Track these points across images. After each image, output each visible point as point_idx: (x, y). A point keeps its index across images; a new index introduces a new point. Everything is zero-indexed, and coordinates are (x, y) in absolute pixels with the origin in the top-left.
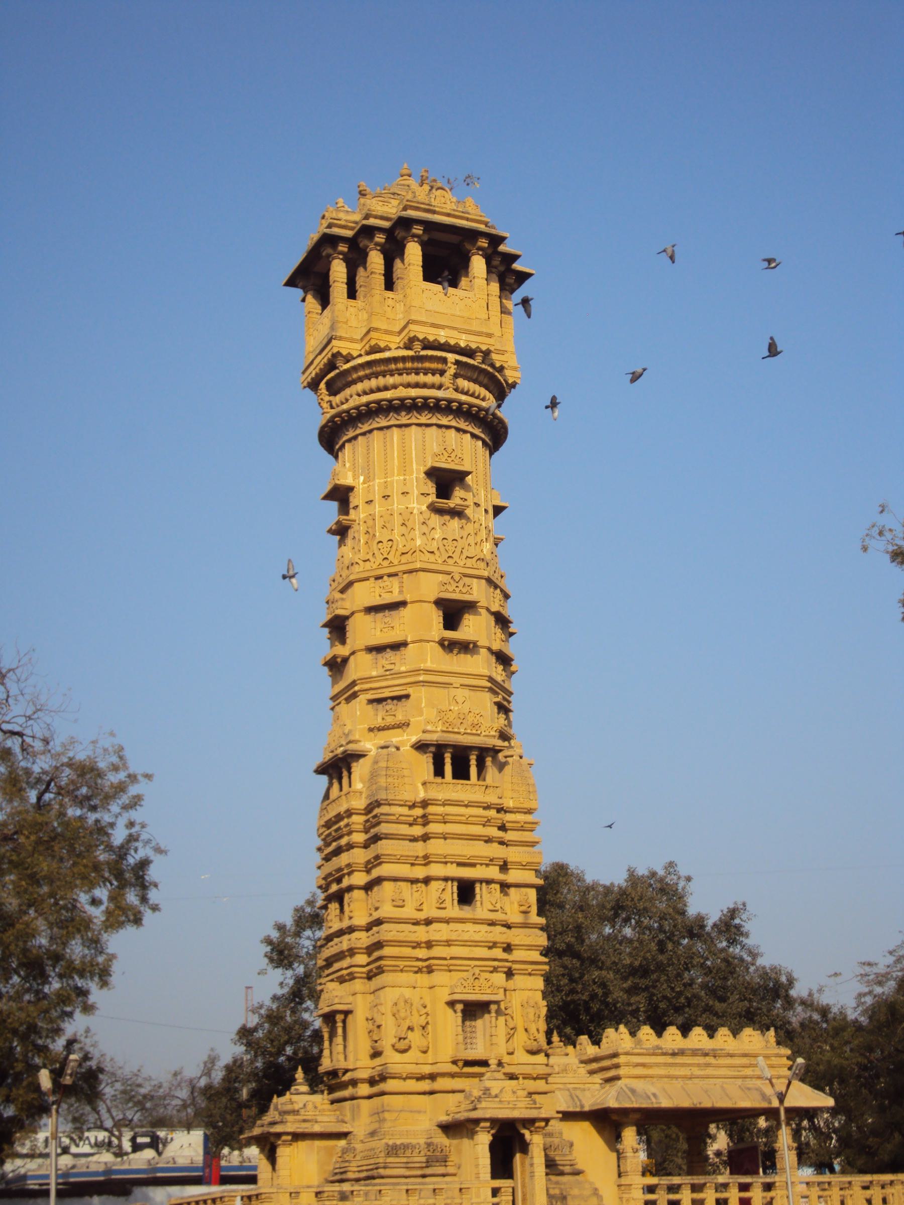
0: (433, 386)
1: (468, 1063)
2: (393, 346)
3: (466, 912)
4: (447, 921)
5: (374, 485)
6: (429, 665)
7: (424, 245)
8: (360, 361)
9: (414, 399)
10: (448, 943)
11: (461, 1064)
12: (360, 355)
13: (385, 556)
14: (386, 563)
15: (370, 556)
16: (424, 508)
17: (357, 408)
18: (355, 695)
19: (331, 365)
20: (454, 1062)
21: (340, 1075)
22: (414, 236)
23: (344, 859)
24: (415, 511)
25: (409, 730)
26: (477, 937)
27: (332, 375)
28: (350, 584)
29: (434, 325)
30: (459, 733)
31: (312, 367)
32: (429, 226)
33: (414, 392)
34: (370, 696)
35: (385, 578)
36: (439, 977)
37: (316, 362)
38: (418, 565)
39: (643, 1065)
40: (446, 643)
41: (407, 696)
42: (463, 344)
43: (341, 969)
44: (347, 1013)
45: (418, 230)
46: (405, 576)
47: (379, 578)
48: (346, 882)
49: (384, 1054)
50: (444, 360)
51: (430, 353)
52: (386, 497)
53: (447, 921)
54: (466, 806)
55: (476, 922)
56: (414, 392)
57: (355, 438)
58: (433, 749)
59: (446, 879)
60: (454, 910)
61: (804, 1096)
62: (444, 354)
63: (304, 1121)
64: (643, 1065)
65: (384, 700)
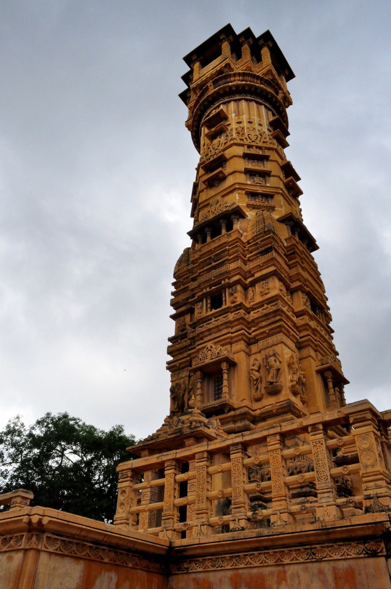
5: (243, 118)
10: (314, 331)
13: (253, 140)
15: (244, 138)
18: (231, 192)
21: (226, 411)
28: (231, 146)
35: (254, 147)
44: (232, 365)
46: (266, 150)
49: (283, 392)
52: (250, 122)
57: (229, 102)
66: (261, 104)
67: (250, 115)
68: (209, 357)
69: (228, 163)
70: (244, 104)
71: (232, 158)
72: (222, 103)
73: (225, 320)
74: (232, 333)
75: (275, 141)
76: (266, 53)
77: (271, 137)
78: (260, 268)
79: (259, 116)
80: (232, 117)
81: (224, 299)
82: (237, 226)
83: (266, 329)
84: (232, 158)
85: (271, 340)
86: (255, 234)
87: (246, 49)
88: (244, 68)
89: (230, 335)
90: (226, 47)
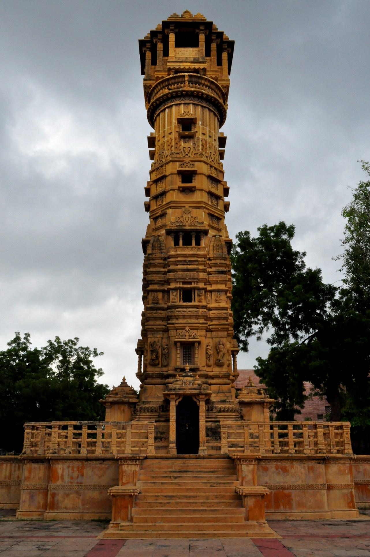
15: (208, 155)
17: (208, 95)
18: (199, 208)
19: (196, 71)
23: (202, 275)
27: (195, 74)
31: (181, 64)
37: (185, 64)
43: (198, 323)
44: (199, 343)
47: (211, 166)
48: (193, 285)
57: (198, 105)
67: (210, 129)
68: (187, 336)
69: (196, 176)
70: (207, 112)
71: (201, 174)
72: (193, 104)
73: (195, 314)
74: (201, 324)
78: (217, 282)
80: (199, 123)
81: (193, 296)
82: (204, 242)
83: (220, 327)
84: (201, 174)
85: (220, 334)
86: (215, 256)
87: (214, 46)
88: (214, 76)
89: (201, 325)
90: (202, 37)
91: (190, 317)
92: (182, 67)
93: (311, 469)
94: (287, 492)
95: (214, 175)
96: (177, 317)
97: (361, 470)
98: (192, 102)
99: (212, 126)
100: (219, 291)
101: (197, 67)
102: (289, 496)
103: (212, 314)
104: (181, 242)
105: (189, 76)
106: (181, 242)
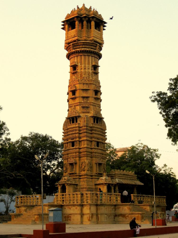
0: (94, 49)
1: (99, 174)
2: (88, 40)
3: (98, 148)
4: (95, 149)
6: (93, 102)
7: (95, 22)
8: (82, 42)
9: (92, 51)
10: (96, 153)
11: (98, 174)
12: (81, 40)
14: (85, 81)
16: (92, 72)
19: (75, 41)
20: (97, 174)
22: (94, 20)
24: (90, 72)
25: (89, 113)
26: (100, 152)
27: (75, 43)
29: (96, 38)
30: (97, 115)
31: (69, 40)
32: (97, 19)
33: (92, 50)
34: (81, 106)
36: (94, 159)
38: (92, 83)
39: (119, 176)
40: (96, 98)
41: (89, 107)
42: (100, 42)
45: (95, 19)
48: (75, 140)
50: (97, 45)
51: (95, 43)
53: (95, 149)
54: (98, 128)
55: (99, 149)
56: (92, 50)
58: (94, 117)
59: (95, 141)
60: (96, 147)
61: (139, 183)
62: (97, 43)
63: (71, 182)
64: (119, 176)
65: (85, 107)
66: (89, 56)
75: (94, 75)
76: (93, 23)
77: (92, 73)
79: (89, 64)
87: (85, 23)
91: (73, 153)
92: (69, 42)
93: (76, 208)
94: (70, 216)
95: (85, 88)
96: (70, 153)
97: (124, 209)
98: (75, 56)
99: (87, 62)
100: (84, 140)
101: (74, 40)
102: (71, 217)
103: (81, 150)
104: (71, 122)
105: (73, 44)
106: (71, 122)
